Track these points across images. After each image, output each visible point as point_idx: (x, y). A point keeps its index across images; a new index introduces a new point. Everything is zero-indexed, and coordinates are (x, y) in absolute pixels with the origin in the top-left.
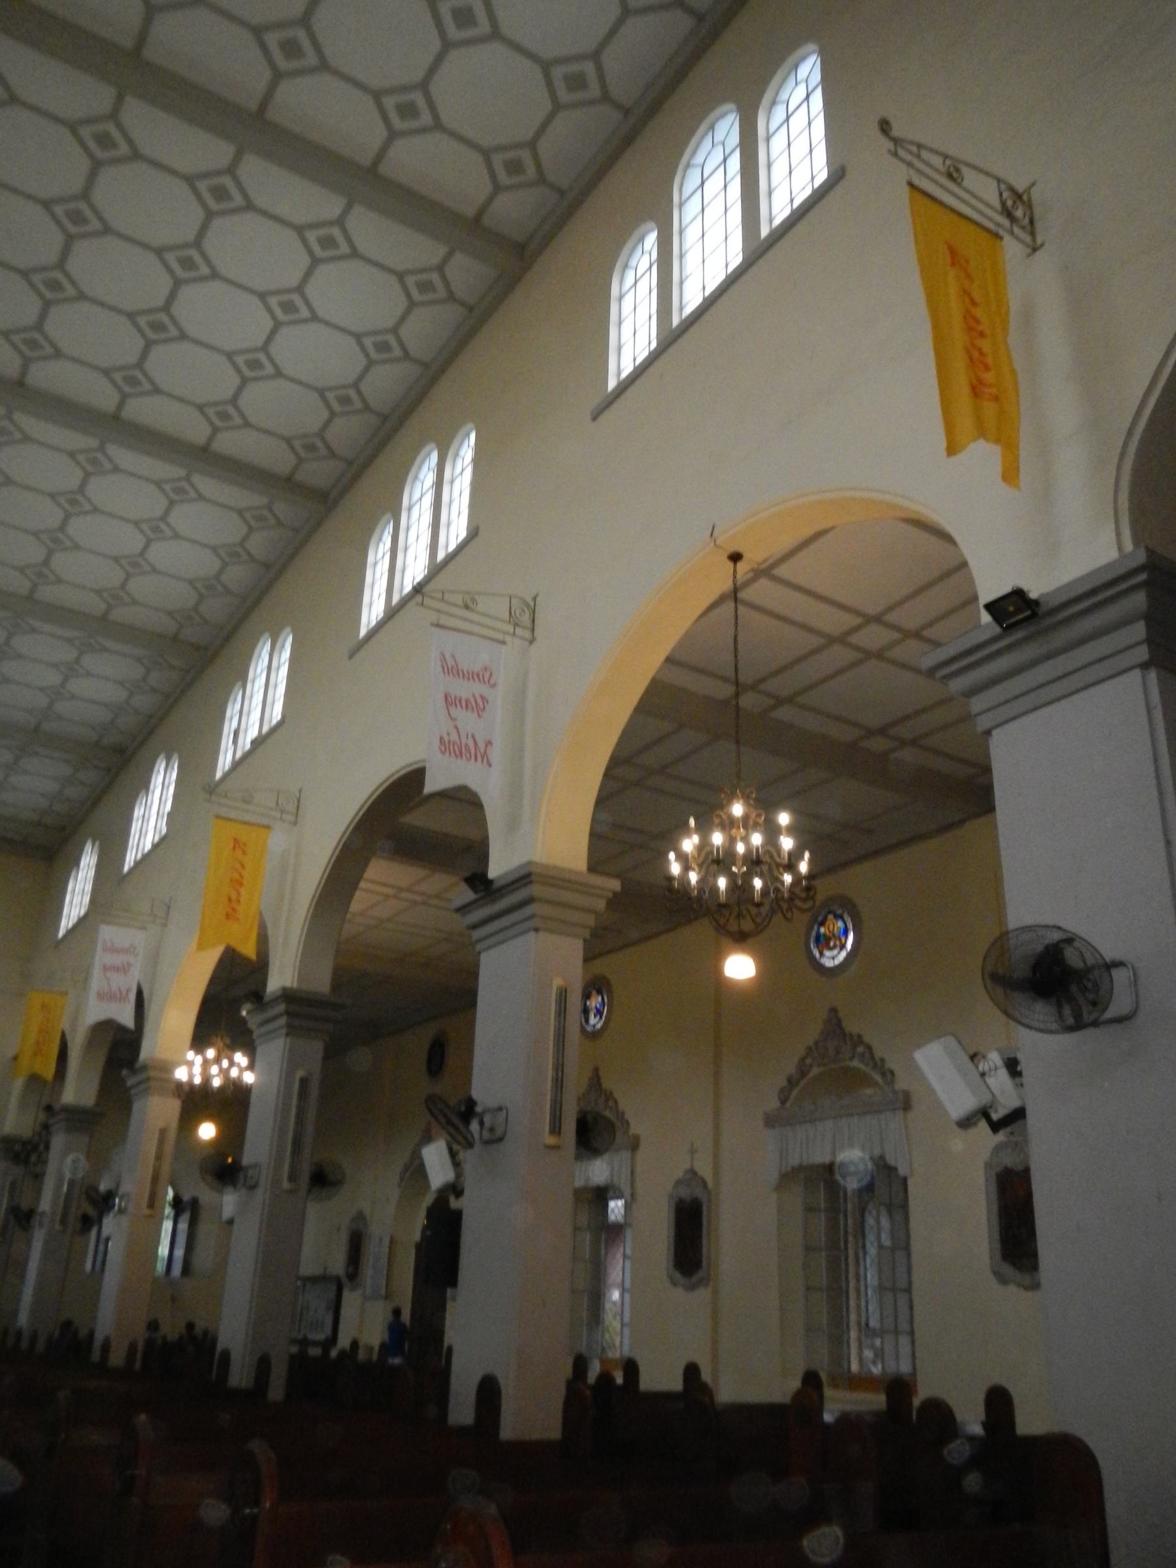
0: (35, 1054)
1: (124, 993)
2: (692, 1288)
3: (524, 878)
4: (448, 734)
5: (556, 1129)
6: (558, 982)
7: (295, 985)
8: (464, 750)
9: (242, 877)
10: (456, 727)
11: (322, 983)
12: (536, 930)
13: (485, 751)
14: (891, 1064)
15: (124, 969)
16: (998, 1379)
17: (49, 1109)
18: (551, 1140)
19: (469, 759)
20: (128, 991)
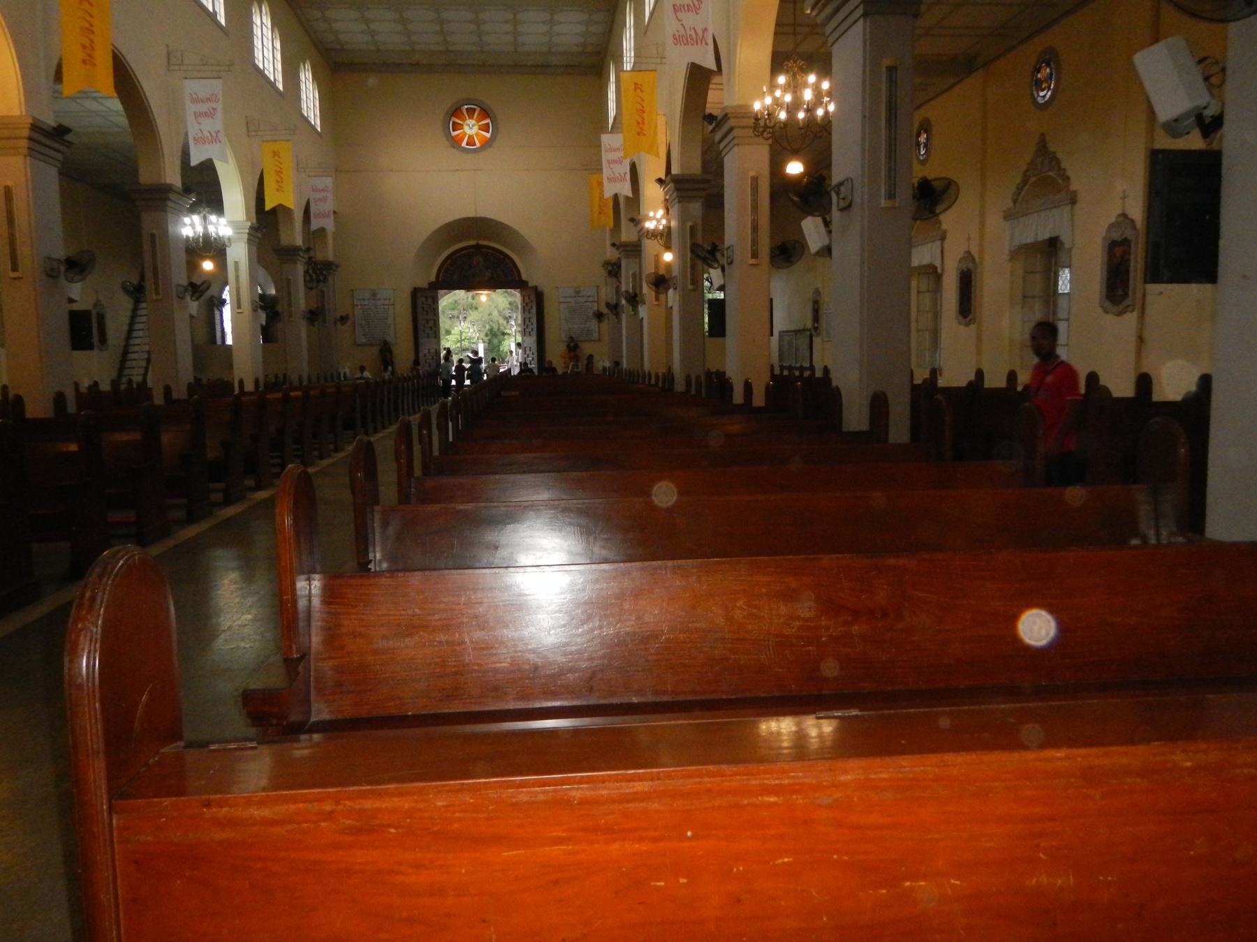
0: (600, 213)
2: (967, 325)
3: (726, 117)
4: (678, 31)
5: (755, 255)
6: (752, 174)
7: (680, 173)
8: (689, 39)
9: (643, 107)
10: (682, 25)
12: (738, 145)
13: (703, 36)
14: (1069, 173)
15: (619, 161)
16: (1096, 369)
19: (692, 45)
20: (625, 173)
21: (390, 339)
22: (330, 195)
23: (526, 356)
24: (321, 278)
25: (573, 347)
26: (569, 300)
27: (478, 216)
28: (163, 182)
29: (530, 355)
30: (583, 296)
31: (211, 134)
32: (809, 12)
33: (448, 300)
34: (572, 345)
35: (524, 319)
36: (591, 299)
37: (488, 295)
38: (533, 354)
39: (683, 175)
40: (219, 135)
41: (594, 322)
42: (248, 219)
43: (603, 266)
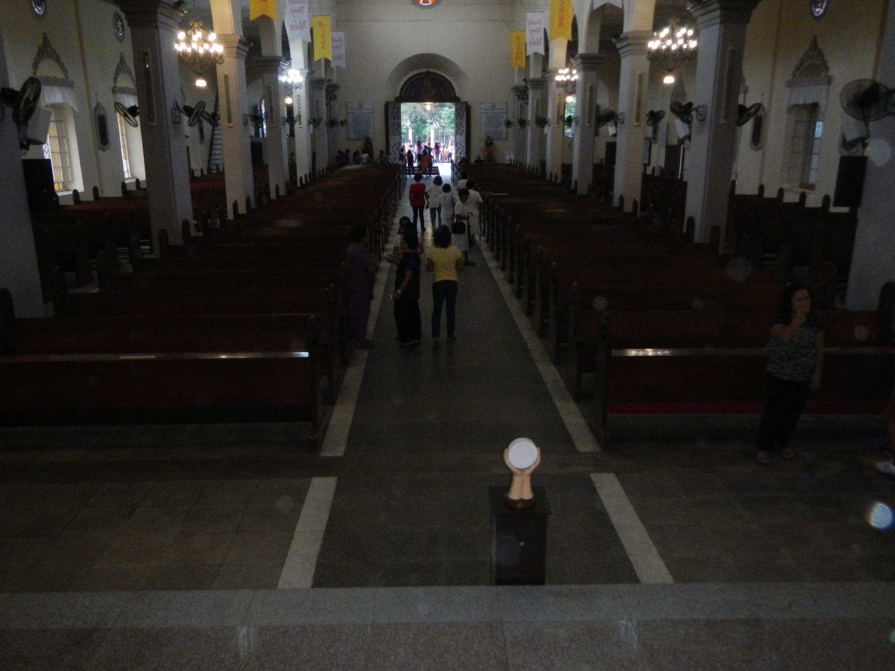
1: (539, 40)
2: (757, 150)
5: (638, 120)
6: (639, 72)
11: (595, 49)
15: (537, 31)
17: (525, 80)
18: (636, 124)
20: (541, 39)
21: (371, 136)
22: (343, 44)
23: (457, 148)
24: (333, 97)
25: (489, 143)
26: (487, 111)
27: (430, 52)
28: (275, 55)
29: (460, 149)
30: (497, 109)
31: (301, 24)
32: (689, 9)
33: (406, 108)
34: (489, 142)
35: (457, 123)
36: (502, 111)
37: (431, 105)
38: (463, 147)
39: (587, 54)
40: (305, 24)
41: (503, 128)
42: (305, 68)
43: (512, 89)
